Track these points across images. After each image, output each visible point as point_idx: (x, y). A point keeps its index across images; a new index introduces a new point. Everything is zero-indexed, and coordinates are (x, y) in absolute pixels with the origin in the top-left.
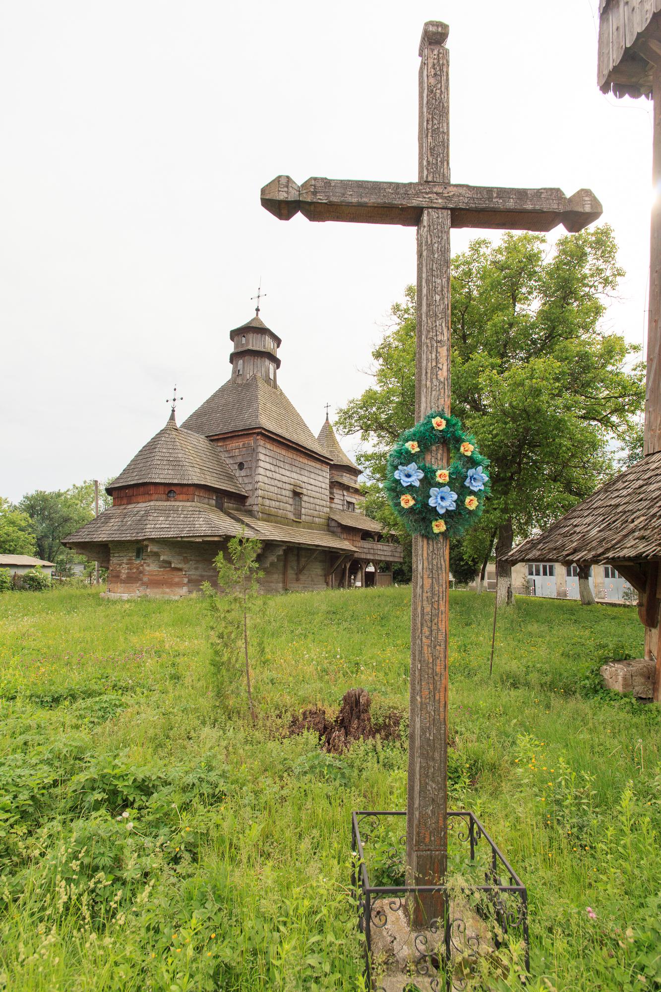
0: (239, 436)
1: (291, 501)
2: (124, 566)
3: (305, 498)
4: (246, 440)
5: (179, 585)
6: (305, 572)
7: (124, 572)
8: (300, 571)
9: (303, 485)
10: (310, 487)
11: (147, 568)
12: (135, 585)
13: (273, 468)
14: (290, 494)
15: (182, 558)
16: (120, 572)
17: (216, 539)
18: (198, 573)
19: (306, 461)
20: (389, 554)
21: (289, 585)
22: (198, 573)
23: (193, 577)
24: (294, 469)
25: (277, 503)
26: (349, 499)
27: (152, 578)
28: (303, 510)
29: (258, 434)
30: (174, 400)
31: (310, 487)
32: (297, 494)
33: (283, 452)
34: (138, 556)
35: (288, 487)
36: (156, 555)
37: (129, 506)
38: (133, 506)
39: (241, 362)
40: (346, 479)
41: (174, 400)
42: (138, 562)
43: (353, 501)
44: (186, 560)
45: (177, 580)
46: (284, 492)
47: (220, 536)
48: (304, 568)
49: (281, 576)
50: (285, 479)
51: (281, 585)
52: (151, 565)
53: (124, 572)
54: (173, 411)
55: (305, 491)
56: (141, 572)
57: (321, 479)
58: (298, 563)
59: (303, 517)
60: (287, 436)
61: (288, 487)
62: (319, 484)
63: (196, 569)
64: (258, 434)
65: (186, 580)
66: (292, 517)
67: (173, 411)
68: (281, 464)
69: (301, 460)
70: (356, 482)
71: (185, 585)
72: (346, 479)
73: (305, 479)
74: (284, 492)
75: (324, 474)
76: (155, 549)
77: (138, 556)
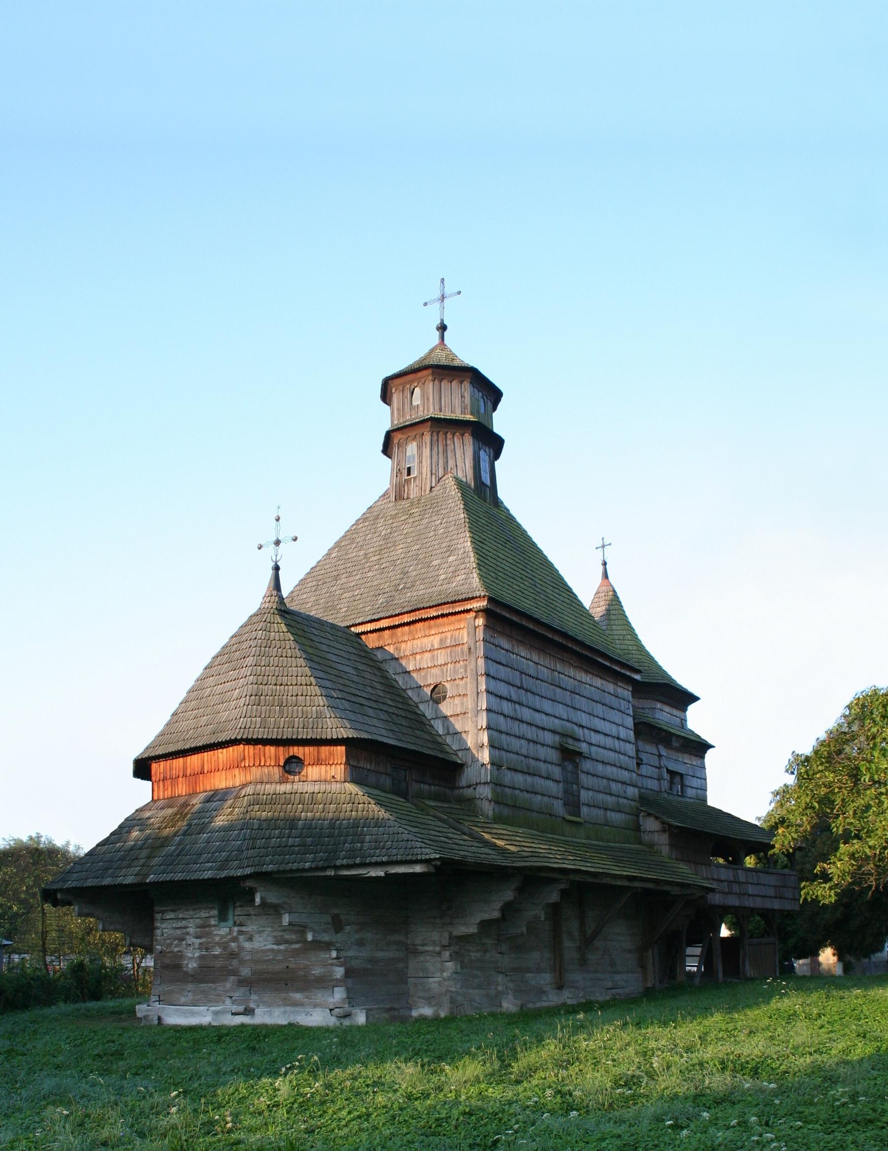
1: (557, 772)
2: (190, 940)
5: (324, 983)
6: (598, 943)
8: (587, 942)
9: (579, 732)
10: (595, 738)
11: (247, 945)
12: (220, 987)
13: (513, 693)
14: (553, 755)
16: (180, 956)
17: (418, 869)
18: (365, 953)
22: (365, 953)
23: (355, 964)
25: (529, 779)
26: (672, 767)
27: (259, 967)
28: (585, 795)
30: (278, 543)
31: (595, 738)
32: (570, 755)
40: (663, 715)
42: (224, 931)
44: (337, 925)
45: (317, 971)
46: (542, 752)
47: (427, 861)
48: (596, 934)
49: (547, 955)
50: (539, 719)
52: (257, 937)
54: (277, 568)
55: (584, 747)
56: (233, 955)
57: (615, 716)
58: (582, 924)
59: (584, 810)
60: (537, 614)
61: (549, 738)
62: (614, 730)
63: (360, 943)
65: (339, 972)
66: (558, 807)
67: (277, 568)
69: (572, 672)
70: (684, 721)
71: (337, 983)
72: (663, 715)
73: (584, 719)
74: (542, 752)
75: (623, 705)
76: (273, 898)
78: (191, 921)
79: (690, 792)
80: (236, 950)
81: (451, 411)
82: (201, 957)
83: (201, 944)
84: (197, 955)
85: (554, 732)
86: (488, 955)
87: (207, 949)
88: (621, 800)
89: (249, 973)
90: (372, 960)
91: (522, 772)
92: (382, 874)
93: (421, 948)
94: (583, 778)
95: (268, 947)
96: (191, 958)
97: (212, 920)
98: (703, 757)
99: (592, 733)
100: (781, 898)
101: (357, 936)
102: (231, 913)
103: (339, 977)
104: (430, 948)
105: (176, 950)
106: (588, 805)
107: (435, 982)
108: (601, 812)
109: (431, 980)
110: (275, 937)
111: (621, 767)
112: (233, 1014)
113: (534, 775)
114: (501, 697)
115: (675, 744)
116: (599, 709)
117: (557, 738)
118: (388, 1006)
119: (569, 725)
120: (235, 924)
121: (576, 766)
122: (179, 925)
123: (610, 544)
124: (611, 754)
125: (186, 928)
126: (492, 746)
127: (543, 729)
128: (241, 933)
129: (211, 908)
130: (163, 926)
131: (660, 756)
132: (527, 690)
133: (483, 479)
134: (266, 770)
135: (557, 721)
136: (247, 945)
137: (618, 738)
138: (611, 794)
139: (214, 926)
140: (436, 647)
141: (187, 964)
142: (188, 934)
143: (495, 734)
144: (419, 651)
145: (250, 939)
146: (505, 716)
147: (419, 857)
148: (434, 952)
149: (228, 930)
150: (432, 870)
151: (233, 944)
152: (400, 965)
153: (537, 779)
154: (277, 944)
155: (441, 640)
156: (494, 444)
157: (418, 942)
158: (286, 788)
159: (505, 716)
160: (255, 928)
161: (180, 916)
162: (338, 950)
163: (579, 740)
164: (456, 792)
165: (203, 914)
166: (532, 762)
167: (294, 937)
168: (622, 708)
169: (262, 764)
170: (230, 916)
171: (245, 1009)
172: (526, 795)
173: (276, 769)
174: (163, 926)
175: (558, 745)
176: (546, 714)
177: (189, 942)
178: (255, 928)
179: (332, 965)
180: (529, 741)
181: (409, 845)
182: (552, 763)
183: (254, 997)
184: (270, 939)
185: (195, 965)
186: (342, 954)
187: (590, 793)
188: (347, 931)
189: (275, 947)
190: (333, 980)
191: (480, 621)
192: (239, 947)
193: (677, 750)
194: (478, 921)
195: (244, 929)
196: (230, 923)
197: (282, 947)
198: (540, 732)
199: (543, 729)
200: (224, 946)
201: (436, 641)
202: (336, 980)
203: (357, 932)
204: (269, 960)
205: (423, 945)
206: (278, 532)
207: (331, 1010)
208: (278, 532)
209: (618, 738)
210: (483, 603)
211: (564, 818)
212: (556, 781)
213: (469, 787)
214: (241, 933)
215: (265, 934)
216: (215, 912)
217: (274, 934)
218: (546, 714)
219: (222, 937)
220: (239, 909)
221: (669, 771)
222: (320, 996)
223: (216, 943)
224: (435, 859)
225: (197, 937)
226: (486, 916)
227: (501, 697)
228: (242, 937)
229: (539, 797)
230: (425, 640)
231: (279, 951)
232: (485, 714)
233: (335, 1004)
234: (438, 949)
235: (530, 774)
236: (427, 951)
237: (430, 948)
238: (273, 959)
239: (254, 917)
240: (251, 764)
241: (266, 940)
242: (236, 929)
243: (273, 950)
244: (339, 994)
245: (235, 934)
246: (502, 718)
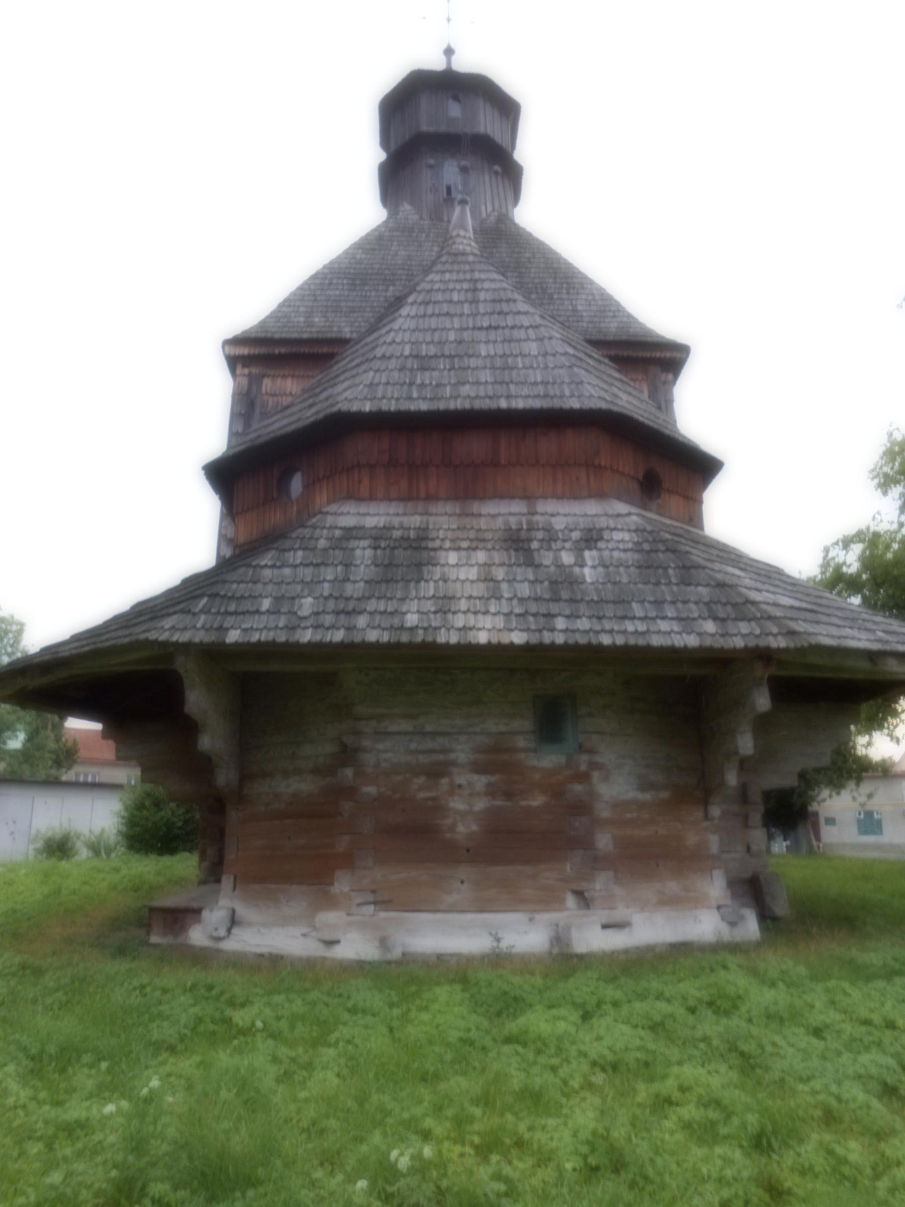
7: (466, 804)
16: (437, 807)
53: (466, 804)
83: (488, 785)
84: (480, 805)
87: (509, 795)
105: (422, 795)
112: (605, 927)
120: (581, 749)
139: (525, 750)
142: (453, 763)
149: (562, 760)
151: (578, 788)
161: (429, 728)
174: (380, 746)
177: (461, 780)
189: (640, 796)
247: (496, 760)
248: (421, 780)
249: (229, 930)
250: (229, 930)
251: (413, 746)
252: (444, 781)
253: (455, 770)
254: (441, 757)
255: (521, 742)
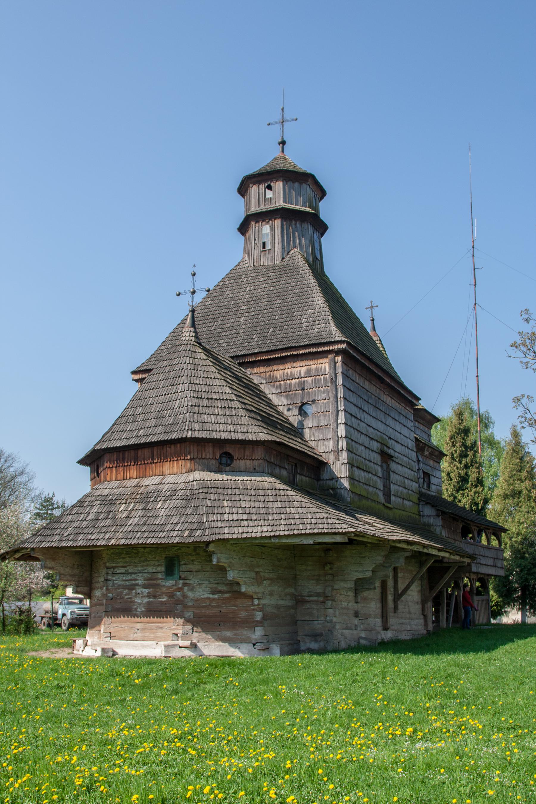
0: (298, 356)
3: (393, 466)
4: (314, 365)
5: (250, 624)
9: (390, 442)
10: (398, 447)
11: (190, 594)
14: (377, 458)
15: (253, 575)
17: (338, 539)
19: (388, 400)
20: (490, 562)
21: (392, 621)
23: (268, 609)
24: (380, 416)
25: (367, 475)
27: (198, 611)
29: (338, 353)
31: (398, 447)
33: (366, 384)
34: (169, 572)
35: (376, 446)
36: (222, 570)
37: (146, 481)
38: (156, 480)
39: (266, 229)
41: (193, 293)
42: (170, 583)
43: (428, 470)
44: (258, 580)
45: (243, 614)
51: (379, 621)
53: (141, 600)
57: (406, 432)
59: (393, 498)
61: (376, 446)
63: (271, 594)
64: (338, 353)
65: (259, 616)
68: (365, 407)
70: (430, 436)
71: (259, 624)
77: (169, 572)
78: (140, 575)
79: (433, 488)
80: (181, 598)
81: (291, 202)
82: (149, 603)
83: (148, 593)
84: (146, 600)
85: (377, 441)
86: (350, 604)
87: (155, 597)
88: (410, 492)
89: (192, 617)
90: (277, 607)
91: (363, 470)
92: (311, 542)
93: (308, 599)
94: (391, 474)
95: (205, 596)
96: (140, 604)
97: (160, 574)
98: (439, 463)
99: (395, 443)
100: (496, 566)
101: (269, 589)
102: (176, 569)
103: (258, 619)
104: (315, 598)
106: (395, 496)
107: (318, 624)
108: (400, 500)
109: (316, 622)
110: (211, 588)
111: (410, 469)
112: (180, 647)
113: (369, 472)
114: (351, 415)
115: (426, 453)
116: (398, 427)
117: (379, 445)
118: (288, 642)
119: (384, 436)
120: (180, 578)
121: (388, 466)
122: (130, 578)
123: (377, 306)
124: (406, 459)
125: (138, 580)
126: (348, 450)
127: (372, 439)
128: (185, 584)
129: (158, 565)
130: (114, 578)
131: (418, 461)
132: (363, 411)
133: (316, 254)
134: (206, 461)
135: (378, 433)
136: (190, 594)
137: (408, 448)
138: (405, 488)
139: (161, 579)
140: (302, 375)
141: (136, 609)
143: (350, 441)
144: (289, 378)
145: (192, 589)
146: (354, 428)
147: (341, 531)
148: (317, 601)
150: (347, 540)
151: (178, 593)
152: (292, 611)
153: (371, 475)
154: (213, 593)
155: (307, 370)
156: (321, 228)
157: (305, 593)
158: (219, 477)
159: (354, 428)
160: (196, 581)
161: (130, 571)
162: (259, 599)
163: (389, 448)
164: (321, 482)
165: (150, 569)
166: (367, 462)
167: (225, 588)
168: (409, 426)
169: (203, 457)
170: (176, 572)
171: (191, 643)
172: (365, 486)
173: (214, 462)
174: (114, 578)
175: (380, 452)
176: (373, 428)
177: (139, 591)
178: (196, 581)
179: (254, 610)
180: (365, 447)
181: (330, 521)
182: (377, 464)
183: (195, 634)
184: (207, 589)
185: (143, 609)
186: (263, 602)
187: (396, 487)
188: (264, 585)
189: (211, 596)
190: (255, 621)
191: (339, 359)
192: (184, 596)
193: (426, 457)
194: (355, 579)
195: (188, 582)
196: (176, 576)
197: (216, 596)
198: (371, 442)
199: (372, 439)
200: (171, 595)
201: (303, 370)
202: (257, 621)
203: (270, 585)
204: (206, 606)
205: (309, 596)
206: (193, 283)
207: (254, 645)
208: (193, 283)
209: (408, 448)
210: (343, 346)
211: (384, 505)
212: (380, 477)
213: (332, 479)
214: (185, 584)
215: (204, 585)
216: (163, 569)
217: (211, 586)
218: (373, 428)
219: (168, 587)
220: (184, 566)
221: (424, 473)
222: (246, 633)
223: (163, 593)
224: (352, 532)
225: (145, 587)
226: (361, 576)
227: (351, 415)
228: (186, 588)
229: (371, 489)
230: (293, 370)
231: (214, 599)
232: (344, 426)
233: (256, 639)
234: (321, 599)
235: (367, 471)
236: (313, 601)
237: (315, 598)
238: (210, 605)
239: (195, 573)
240: (195, 457)
241: (204, 591)
242: (181, 581)
243: (209, 598)
244: (259, 632)
245: (180, 586)
246: (352, 430)
247: (151, 584)
248: (126, 591)
249: (84, 648)
250: (84, 648)
251: (124, 578)
252: (134, 591)
253: (137, 587)
254: (134, 582)
255: (160, 576)
